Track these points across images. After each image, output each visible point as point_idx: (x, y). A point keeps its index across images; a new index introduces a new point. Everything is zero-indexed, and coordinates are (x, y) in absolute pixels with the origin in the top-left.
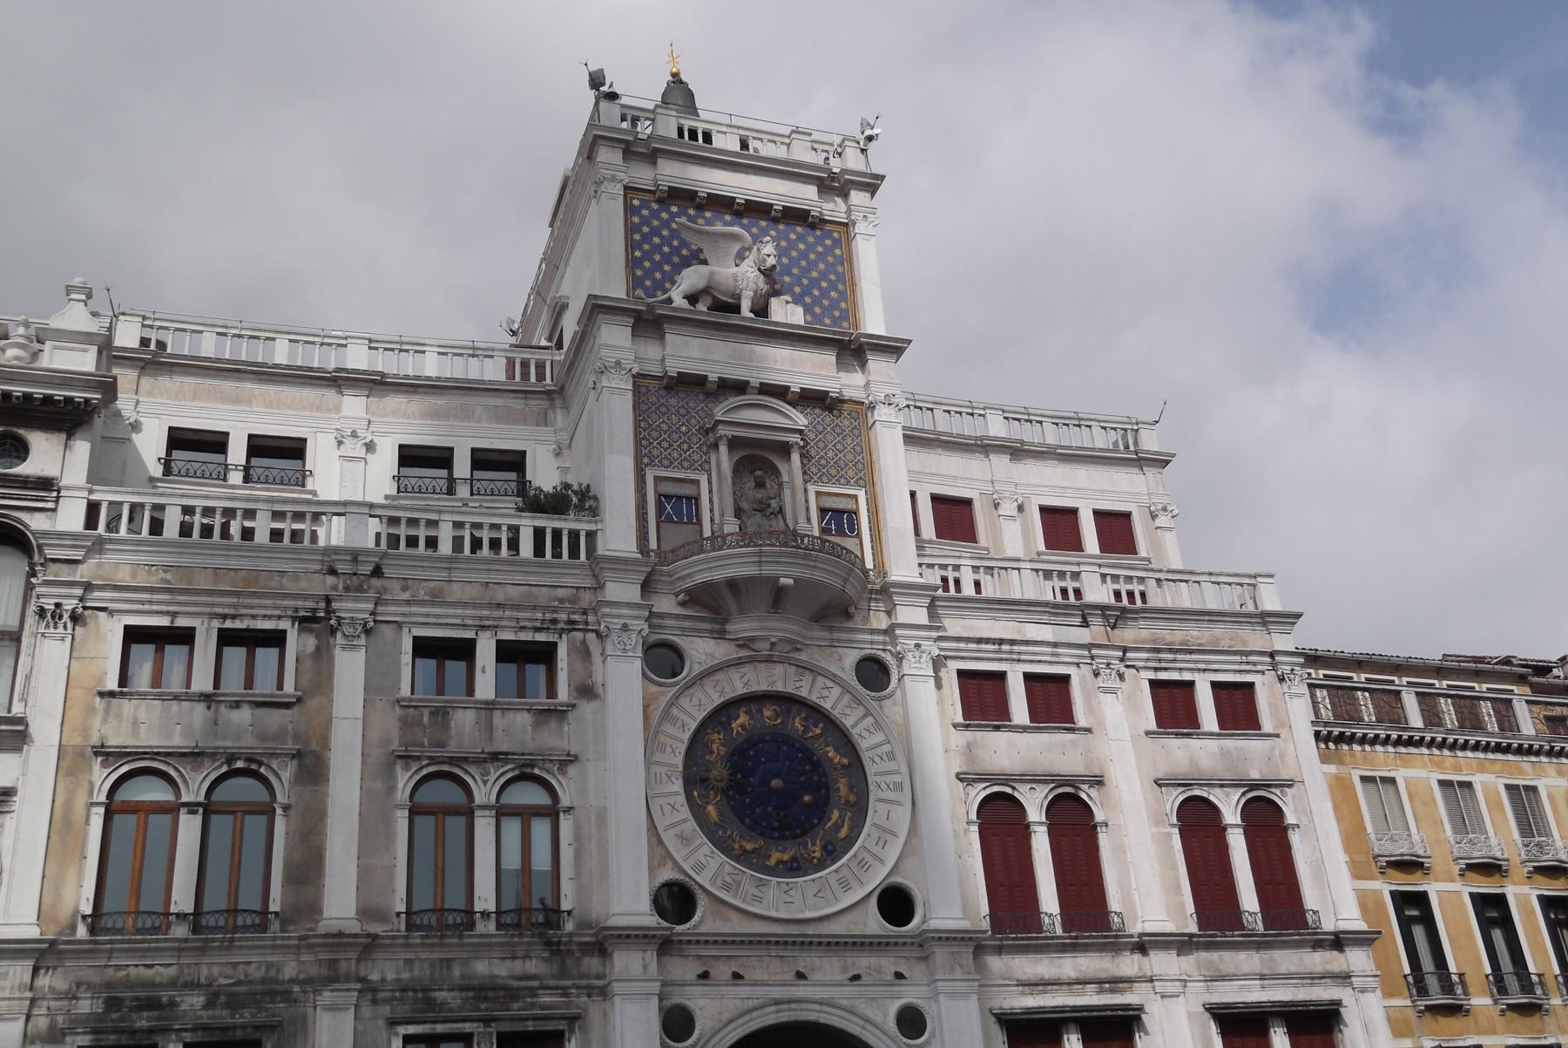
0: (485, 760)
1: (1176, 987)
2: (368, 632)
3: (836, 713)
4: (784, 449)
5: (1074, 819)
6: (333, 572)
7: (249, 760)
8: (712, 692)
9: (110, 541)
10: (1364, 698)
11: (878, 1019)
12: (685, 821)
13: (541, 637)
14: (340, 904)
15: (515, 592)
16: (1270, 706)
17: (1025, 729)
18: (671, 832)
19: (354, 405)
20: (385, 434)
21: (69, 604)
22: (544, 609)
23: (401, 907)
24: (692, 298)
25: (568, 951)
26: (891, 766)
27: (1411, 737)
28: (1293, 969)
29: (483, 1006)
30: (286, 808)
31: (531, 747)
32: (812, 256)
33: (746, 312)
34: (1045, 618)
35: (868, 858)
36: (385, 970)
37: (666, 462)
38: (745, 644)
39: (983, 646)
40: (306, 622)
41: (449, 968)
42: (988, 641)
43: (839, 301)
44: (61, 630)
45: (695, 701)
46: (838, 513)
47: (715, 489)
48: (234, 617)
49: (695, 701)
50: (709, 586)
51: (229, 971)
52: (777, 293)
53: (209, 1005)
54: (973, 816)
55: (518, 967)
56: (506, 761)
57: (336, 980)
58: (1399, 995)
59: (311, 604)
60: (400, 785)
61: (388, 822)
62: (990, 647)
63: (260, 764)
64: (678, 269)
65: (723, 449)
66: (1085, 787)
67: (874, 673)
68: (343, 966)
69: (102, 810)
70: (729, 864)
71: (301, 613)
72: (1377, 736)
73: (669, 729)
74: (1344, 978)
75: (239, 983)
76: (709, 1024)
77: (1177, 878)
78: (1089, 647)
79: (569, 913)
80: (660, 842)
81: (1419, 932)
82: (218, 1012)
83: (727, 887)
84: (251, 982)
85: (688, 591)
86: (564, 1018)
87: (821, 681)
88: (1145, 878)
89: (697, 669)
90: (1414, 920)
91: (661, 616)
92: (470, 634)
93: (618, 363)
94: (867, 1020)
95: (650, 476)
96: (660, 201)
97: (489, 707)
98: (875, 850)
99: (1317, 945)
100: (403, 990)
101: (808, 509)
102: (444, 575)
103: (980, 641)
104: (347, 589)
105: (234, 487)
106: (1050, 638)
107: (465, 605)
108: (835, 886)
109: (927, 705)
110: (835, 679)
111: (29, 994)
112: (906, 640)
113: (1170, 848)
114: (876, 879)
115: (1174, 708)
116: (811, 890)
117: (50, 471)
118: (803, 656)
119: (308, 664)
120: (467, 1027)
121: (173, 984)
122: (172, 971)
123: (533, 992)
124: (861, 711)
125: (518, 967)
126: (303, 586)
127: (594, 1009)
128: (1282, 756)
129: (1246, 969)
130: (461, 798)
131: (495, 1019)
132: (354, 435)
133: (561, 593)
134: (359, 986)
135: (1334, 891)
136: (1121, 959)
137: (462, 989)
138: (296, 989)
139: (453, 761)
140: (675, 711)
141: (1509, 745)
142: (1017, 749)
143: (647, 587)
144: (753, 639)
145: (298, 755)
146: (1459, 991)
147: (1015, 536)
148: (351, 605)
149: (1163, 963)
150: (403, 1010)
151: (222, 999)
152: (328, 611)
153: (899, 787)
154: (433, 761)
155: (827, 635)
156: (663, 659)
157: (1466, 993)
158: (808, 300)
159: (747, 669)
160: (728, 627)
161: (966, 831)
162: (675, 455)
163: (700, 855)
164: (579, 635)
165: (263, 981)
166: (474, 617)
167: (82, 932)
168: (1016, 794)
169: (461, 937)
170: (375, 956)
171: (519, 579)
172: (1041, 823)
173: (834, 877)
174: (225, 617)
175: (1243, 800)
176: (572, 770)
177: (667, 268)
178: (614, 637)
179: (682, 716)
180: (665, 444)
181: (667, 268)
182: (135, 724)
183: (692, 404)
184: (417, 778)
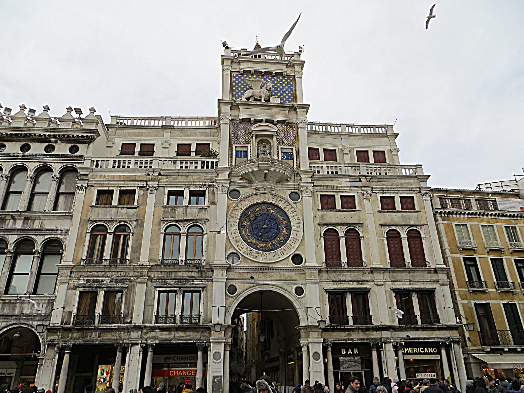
1: (382, 283)
2: (156, 189)
4: (272, 137)
5: (353, 236)
6: (149, 175)
8: (247, 202)
10: (452, 202)
11: (290, 290)
14: (144, 258)
15: (195, 178)
16: (418, 202)
17: (340, 211)
19: (167, 135)
20: (174, 141)
21: (84, 185)
22: (202, 182)
24: (248, 99)
26: (298, 221)
27: (472, 213)
30: (133, 234)
31: (197, 218)
33: (263, 101)
34: (348, 180)
35: (290, 246)
41: (172, 274)
42: (330, 186)
43: (291, 96)
45: (243, 205)
47: (252, 148)
48: (123, 187)
49: (243, 205)
50: (246, 174)
52: (272, 95)
53: (111, 282)
54: (322, 235)
55: (190, 274)
56: (190, 221)
57: (142, 276)
58: (464, 287)
59: (142, 183)
61: (159, 237)
62: (330, 188)
64: (245, 91)
65: (254, 137)
66: (357, 227)
67: (295, 196)
72: (461, 212)
73: (235, 213)
74: (437, 281)
75: (119, 276)
77: (385, 252)
78: (361, 187)
79: (204, 260)
81: (472, 269)
83: (248, 254)
85: (241, 176)
87: (279, 198)
88: (375, 251)
89: (244, 196)
90: (472, 266)
91: (234, 182)
92: (183, 189)
93: (226, 117)
94: (286, 290)
96: (241, 74)
97: (187, 207)
98: (292, 244)
103: (327, 186)
104: (152, 179)
106: (349, 185)
107: (181, 182)
108: (279, 254)
109: (309, 204)
110: (283, 198)
111: (68, 278)
112: (303, 187)
113: (384, 244)
114: (291, 252)
115: (387, 204)
118: (274, 192)
120: (175, 289)
122: (103, 273)
123: (193, 281)
124: (290, 207)
125: (190, 274)
126: (141, 178)
127: (209, 284)
128: (421, 217)
129: (405, 278)
130: (179, 231)
131: (182, 287)
132: (166, 142)
133: (207, 178)
135: (433, 257)
137: (174, 279)
139: (176, 221)
141: (507, 214)
142: (337, 216)
143: (230, 175)
144: (259, 188)
145: (137, 220)
146: (484, 286)
147: (350, 158)
148: (152, 183)
149: (378, 276)
150: (159, 285)
151: (114, 280)
153: (300, 227)
154: (171, 221)
156: (233, 193)
157: (487, 287)
158: (282, 97)
163: (241, 245)
164: (212, 188)
165: (124, 276)
169: (174, 266)
171: (196, 174)
172: (343, 237)
174: (121, 187)
176: (207, 223)
177: (242, 91)
178: (220, 188)
181: (242, 91)
182: (98, 213)
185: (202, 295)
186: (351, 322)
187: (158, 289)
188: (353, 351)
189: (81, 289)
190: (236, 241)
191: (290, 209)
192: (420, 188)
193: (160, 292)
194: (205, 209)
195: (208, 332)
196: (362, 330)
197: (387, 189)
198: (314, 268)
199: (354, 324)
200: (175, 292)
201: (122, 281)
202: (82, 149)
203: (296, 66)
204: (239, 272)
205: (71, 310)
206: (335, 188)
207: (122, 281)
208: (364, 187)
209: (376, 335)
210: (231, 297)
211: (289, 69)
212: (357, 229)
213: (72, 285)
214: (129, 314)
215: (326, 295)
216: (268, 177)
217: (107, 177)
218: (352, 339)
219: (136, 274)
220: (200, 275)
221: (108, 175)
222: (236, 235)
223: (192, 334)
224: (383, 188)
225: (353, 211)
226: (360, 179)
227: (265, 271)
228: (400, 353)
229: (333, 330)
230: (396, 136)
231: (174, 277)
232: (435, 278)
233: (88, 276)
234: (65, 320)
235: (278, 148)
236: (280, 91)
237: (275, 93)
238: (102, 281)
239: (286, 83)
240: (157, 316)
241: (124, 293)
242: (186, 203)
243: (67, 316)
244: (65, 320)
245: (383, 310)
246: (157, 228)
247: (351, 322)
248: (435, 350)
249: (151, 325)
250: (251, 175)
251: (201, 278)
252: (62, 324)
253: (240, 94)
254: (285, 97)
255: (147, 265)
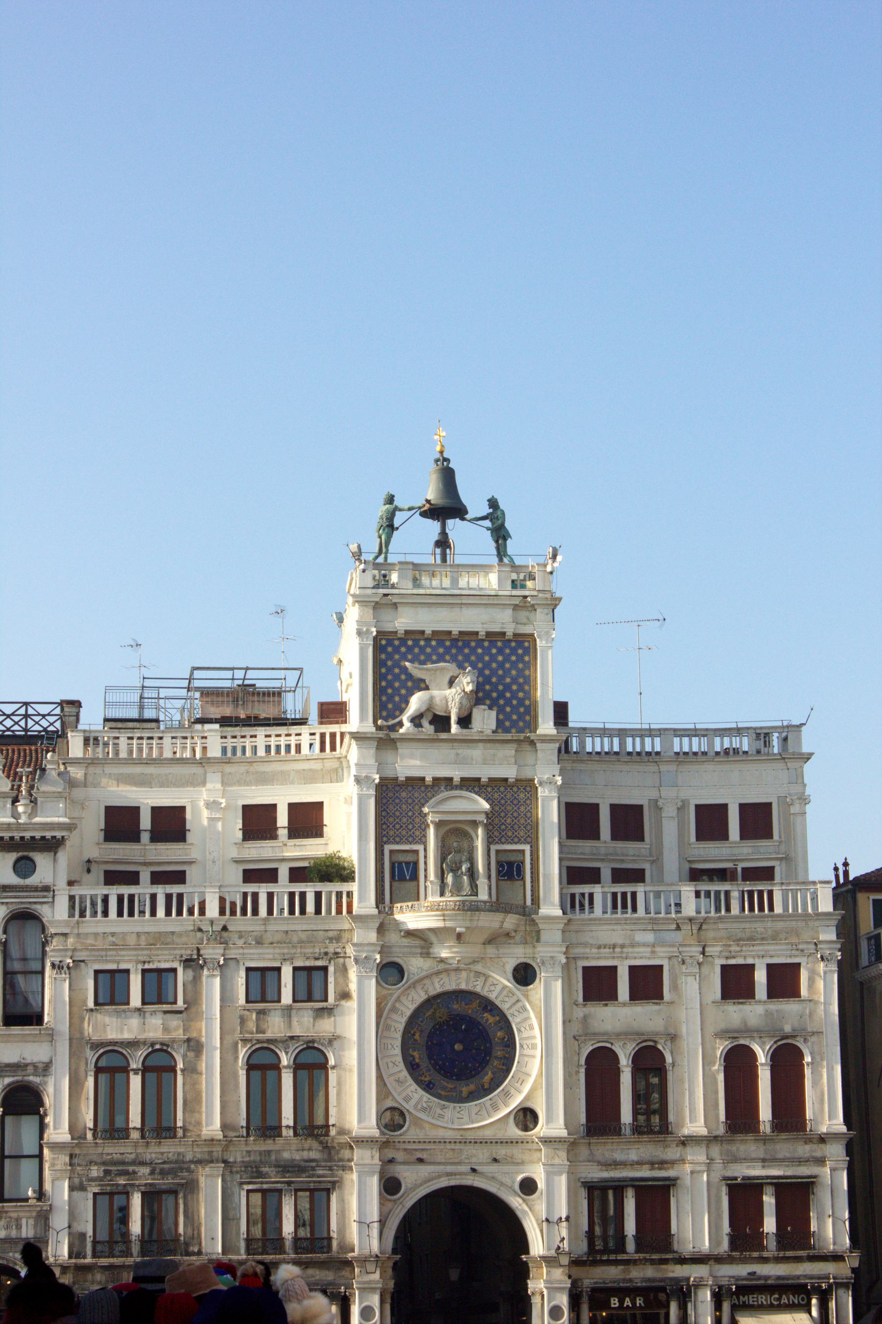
0: (287, 1040)
3: (497, 1002)
4: (474, 824)
5: (651, 1063)
6: (200, 930)
7: (162, 1044)
9: (83, 922)
12: (400, 1071)
13: (319, 963)
15: (303, 936)
17: (624, 1004)
18: (392, 1078)
23: (245, 1125)
24: (416, 720)
25: (334, 1147)
28: (788, 1155)
29: (287, 1175)
30: (182, 1071)
32: (507, 665)
34: (650, 927)
36: (237, 1155)
37: (397, 839)
38: (442, 961)
39: (602, 950)
40: (188, 962)
44: (63, 976)
46: (510, 864)
48: (149, 962)
49: (410, 998)
51: (160, 1156)
52: (478, 702)
53: (152, 1173)
54: (583, 1061)
55: (306, 1155)
57: (212, 1162)
59: (189, 952)
60: (241, 1057)
61: (236, 1075)
62: (607, 950)
63: (168, 1046)
68: (215, 1154)
69: (92, 1073)
70: (426, 1096)
71: (185, 957)
73: (395, 1017)
75: (164, 1163)
76: (409, 1186)
79: (333, 1125)
80: (385, 1084)
82: (156, 1176)
83: (424, 1110)
84: (171, 1162)
86: (330, 1182)
94: (502, 1184)
95: (387, 848)
97: (289, 1008)
99: (808, 1141)
100: (245, 1167)
101: (489, 864)
102: (262, 928)
103: (599, 947)
105: (145, 845)
111: (69, 1168)
115: (736, 983)
116: (475, 1110)
117: (48, 880)
118: (479, 967)
119: (189, 987)
120: (279, 1186)
121: (134, 1163)
122: (133, 1156)
123: (313, 1169)
128: (811, 1015)
129: (754, 1156)
133: (331, 934)
134: (223, 1165)
136: (669, 1149)
137: (275, 1166)
138: (193, 1166)
139: (269, 1041)
140: (397, 1005)
145: (188, 1040)
148: (211, 951)
151: (158, 1171)
152: (199, 955)
155: (495, 951)
156: (391, 971)
158: (502, 702)
159: (444, 976)
160: (431, 950)
161: (578, 1072)
162: (404, 833)
163: (408, 1091)
164: (341, 960)
165: (176, 1162)
166: (279, 954)
167: (89, 1135)
168: (613, 1048)
170: (231, 1149)
171: (305, 927)
173: (490, 1102)
174: (144, 962)
175: (775, 1046)
179: (402, 1008)
180: (398, 826)
183: (416, 795)
184: (250, 1051)
185: (334, 1198)
186: (631, 1246)
187: (246, 1187)
188: (634, 1302)
189: (96, 1190)
190: (398, 1081)
191: (514, 1004)
192: (816, 944)
193: (248, 1191)
194: (329, 1011)
195: (348, 1269)
196: (653, 1262)
197: (738, 949)
198: (559, 1140)
199: (637, 1252)
200: (280, 1191)
201: (173, 1172)
202: (42, 860)
203: (538, 610)
204: (405, 1150)
205: (84, 1231)
206: (618, 950)
207: (173, 1172)
208: (685, 945)
209: (678, 1271)
210: (390, 1200)
211: (523, 615)
212: (660, 1047)
213: (77, 1181)
214: (196, 1237)
215: (583, 1193)
216: (463, 938)
217: (110, 938)
218: (630, 1280)
219: (199, 1156)
220: (326, 1156)
221: (113, 934)
222: (396, 1069)
223: (318, 1272)
224: (730, 946)
225: (656, 1003)
226: (677, 924)
227: (458, 1146)
228: (726, 1306)
229: (595, 1263)
230: (808, 757)
231: (274, 1162)
232: (818, 1154)
233: (104, 1163)
234: (75, 1249)
235: (489, 851)
236: (497, 684)
237: (484, 690)
238: (134, 1172)
239: (514, 658)
240: (249, 1241)
241: (181, 1195)
242: (287, 997)
243: (77, 1242)
244: (75, 1249)
245: (698, 1224)
246: (229, 1057)
247: (631, 1246)
248: (803, 1299)
249: (240, 1257)
250: (427, 932)
251: (329, 1164)
252: (70, 1257)
253: (397, 699)
254: (508, 702)
255: (220, 1140)
